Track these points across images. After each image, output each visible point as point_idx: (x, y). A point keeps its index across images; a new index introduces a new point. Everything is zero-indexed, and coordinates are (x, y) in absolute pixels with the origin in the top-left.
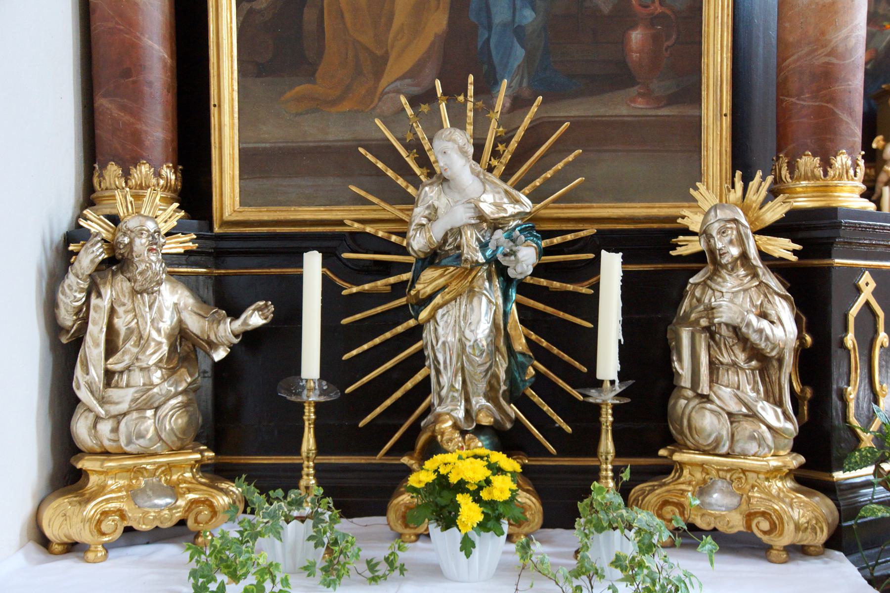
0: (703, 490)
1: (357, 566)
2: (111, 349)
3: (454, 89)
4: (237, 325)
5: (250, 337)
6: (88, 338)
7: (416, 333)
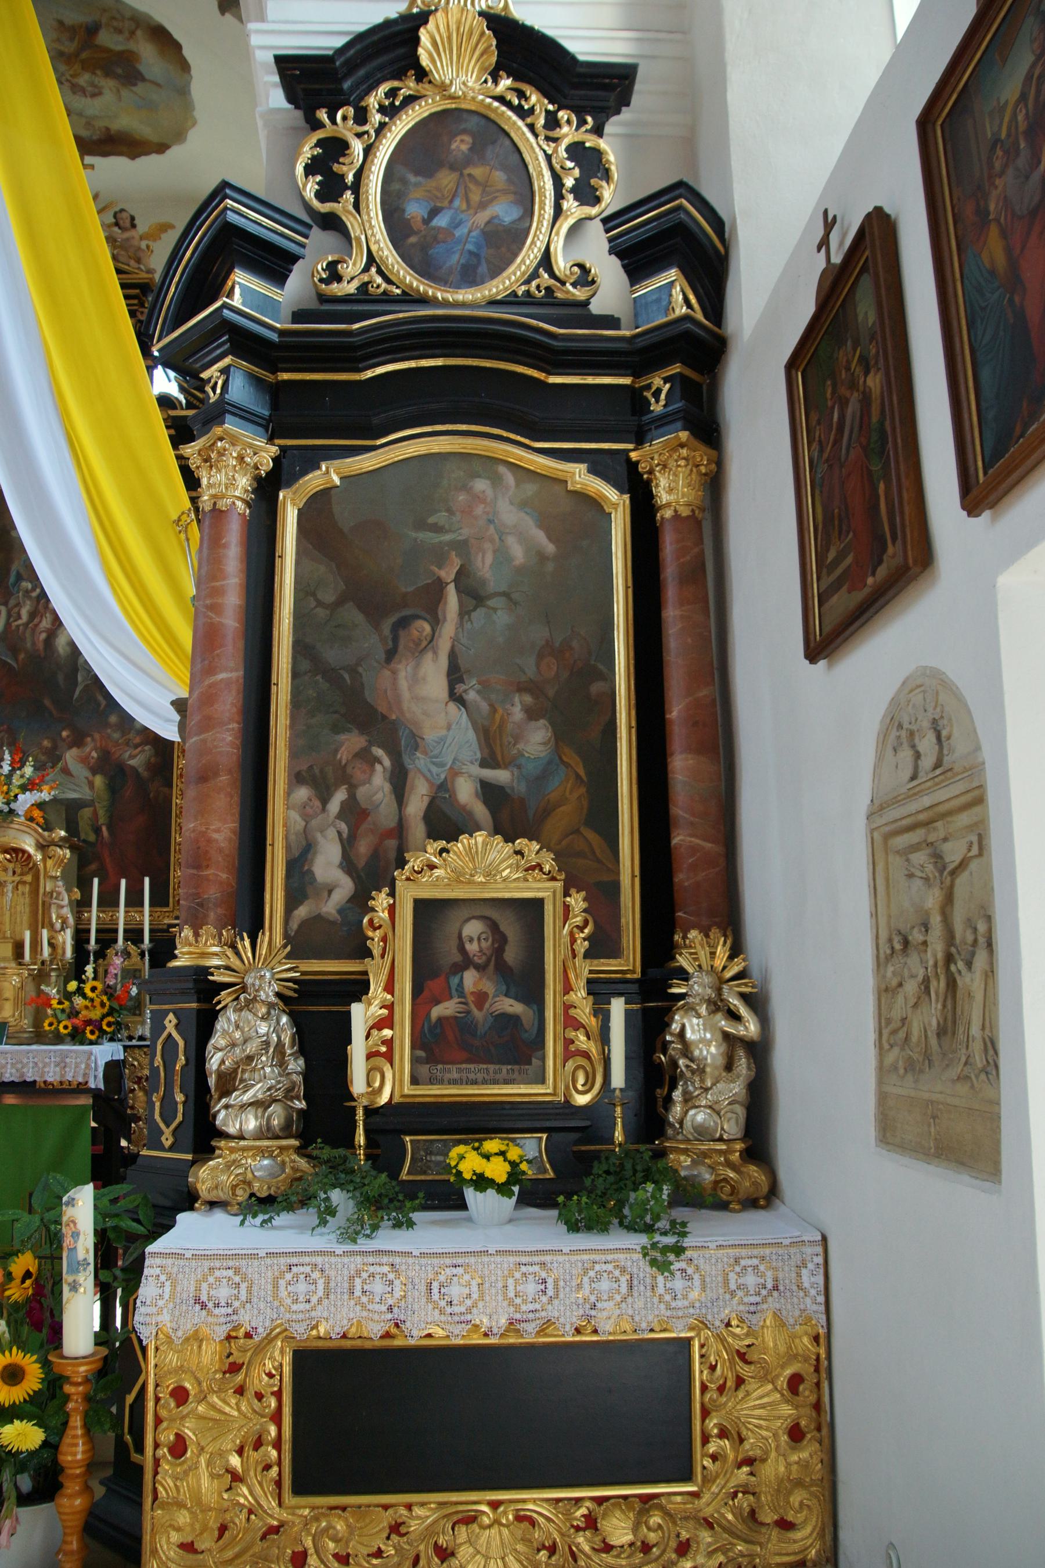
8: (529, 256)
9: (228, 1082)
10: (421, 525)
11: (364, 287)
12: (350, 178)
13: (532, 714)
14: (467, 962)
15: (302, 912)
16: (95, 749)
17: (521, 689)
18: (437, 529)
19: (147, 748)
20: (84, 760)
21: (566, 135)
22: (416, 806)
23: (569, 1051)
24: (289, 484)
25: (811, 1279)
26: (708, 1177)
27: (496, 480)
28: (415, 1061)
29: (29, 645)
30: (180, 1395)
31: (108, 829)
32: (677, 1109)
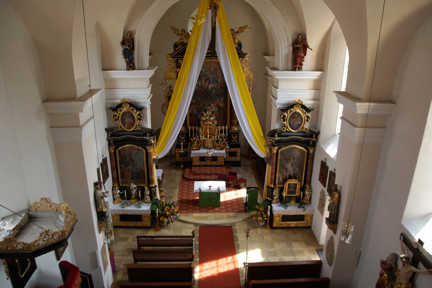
2: (116, 194)
5: (123, 193)
8: (301, 127)
9: (275, 196)
10: (290, 153)
11: (286, 131)
12: (286, 119)
13: (297, 168)
14: (291, 187)
15: (279, 182)
17: (297, 166)
18: (291, 153)
19: (224, 104)
20: (214, 105)
21: (306, 115)
22: (288, 174)
23: (298, 193)
24: (279, 150)
25: (313, 212)
26: (306, 202)
27: (296, 149)
28: (287, 194)
29: (204, 88)
30: (276, 217)
31: (218, 115)
32: (305, 198)
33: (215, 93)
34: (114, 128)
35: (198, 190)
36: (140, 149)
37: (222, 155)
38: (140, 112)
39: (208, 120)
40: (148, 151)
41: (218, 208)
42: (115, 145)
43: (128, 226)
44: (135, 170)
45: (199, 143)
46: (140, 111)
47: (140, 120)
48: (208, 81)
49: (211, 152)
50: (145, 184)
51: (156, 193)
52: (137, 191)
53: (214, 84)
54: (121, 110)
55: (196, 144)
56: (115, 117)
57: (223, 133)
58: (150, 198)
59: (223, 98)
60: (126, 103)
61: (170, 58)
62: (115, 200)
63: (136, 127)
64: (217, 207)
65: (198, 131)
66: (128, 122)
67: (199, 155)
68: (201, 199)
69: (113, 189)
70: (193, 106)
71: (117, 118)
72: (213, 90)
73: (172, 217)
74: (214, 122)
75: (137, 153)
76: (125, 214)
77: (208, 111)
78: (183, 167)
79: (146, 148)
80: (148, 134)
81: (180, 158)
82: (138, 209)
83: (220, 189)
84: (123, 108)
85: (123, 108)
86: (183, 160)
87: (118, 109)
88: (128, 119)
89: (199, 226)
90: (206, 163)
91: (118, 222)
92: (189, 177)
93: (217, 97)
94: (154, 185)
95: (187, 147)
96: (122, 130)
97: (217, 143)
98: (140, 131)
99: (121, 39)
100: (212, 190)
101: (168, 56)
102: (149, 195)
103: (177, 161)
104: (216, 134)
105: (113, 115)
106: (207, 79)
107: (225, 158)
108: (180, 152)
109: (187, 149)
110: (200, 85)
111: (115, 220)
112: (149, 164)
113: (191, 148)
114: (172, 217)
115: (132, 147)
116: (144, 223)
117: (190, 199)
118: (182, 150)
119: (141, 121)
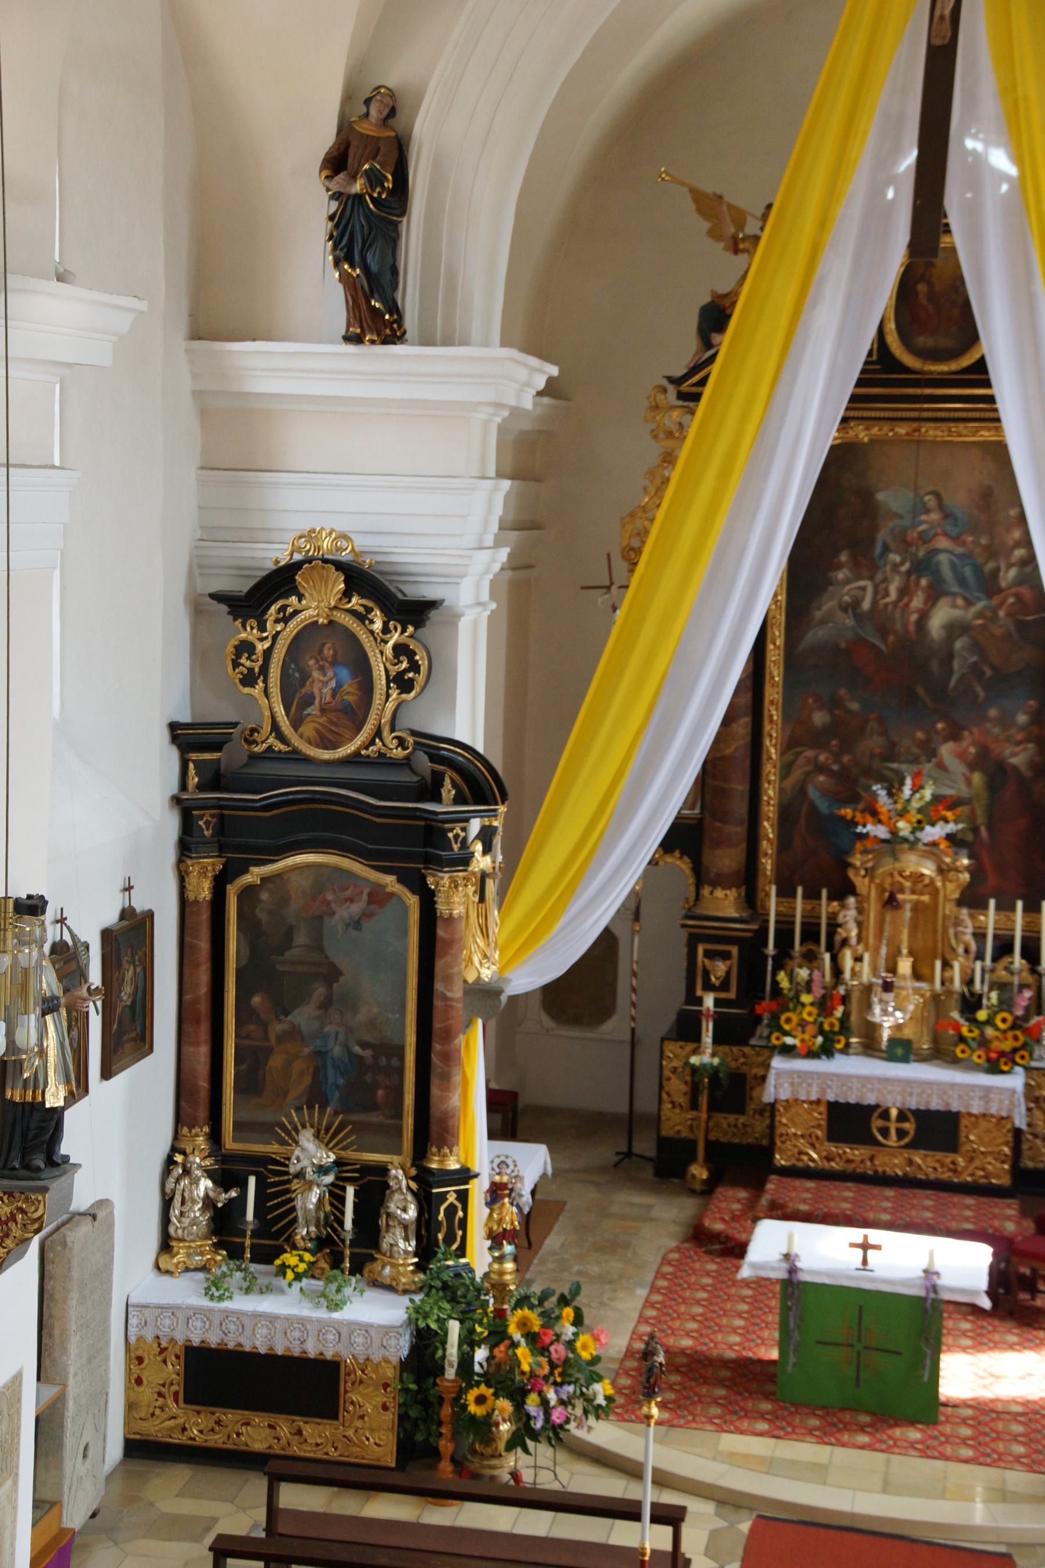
0: (383, 1267)
1: (256, 1288)
2: (183, 1203)
3: (311, 1108)
4: (227, 1196)
5: (231, 1200)
6: (175, 1201)
7: (292, 1200)
16: (974, 743)
19: (1031, 745)
20: (961, 755)
29: (898, 626)
33: (975, 664)
34: (235, 725)
35: (775, 1265)
36: (389, 889)
37: (1000, 1109)
38: (411, 636)
39: (905, 840)
40: (441, 907)
41: (920, 1426)
42: (222, 849)
43: (230, 1446)
44: (341, 1037)
45: (834, 1008)
46: (411, 629)
47: (405, 685)
48: (924, 582)
49: (892, 1014)
50: (398, 1151)
51: (463, 1224)
52: (337, 1197)
53: (969, 603)
54: (290, 610)
55: (808, 1009)
56: (243, 661)
57: (1017, 960)
58: (416, 1255)
59: (1032, 703)
60: (325, 561)
61: (675, 414)
62: (173, 1243)
63: (378, 733)
64: (912, 1423)
65: (834, 925)
66: (328, 698)
67: (823, 1091)
68: (796, 1335)
69: (170, 1162)
70: (809, 753)
71: (260, 663)
72: (959, 644)
73: (556, 1392)
74: (948, 860)
75: (366, 915)
76: (223, 1343)
77: (908, 782)
78: (705, 1175)
79: (430, 880)
80: (447, 782)
81: (690, 1115)
82: (322, 1314)
83: (937, 1274)
84: (300, 601)
85: (300, 601)
86: (707, 1131)
87: (268, 608)
88: (325, 676)
89: (754, 1515)
90: (872, 1159)
91: (162, 1408)
92: (730, 1232)
93: (982, 694)
94: (458, 1161)
95: (752, 1034)
96: (280, 752)
97: (962, 1021)
98: (402, 765)
99: (326, 137)
100: (879, 1273)
101: (661, 397)
102: (413, 1228)
103: (664, 1133)
104: (961, 950)
105: (236, 647)
106: (923, 566)
107: (1017, 1133)
108: (694, 1060)
109: (747, 1050)
110: (866, 605)
111: (146, 1394)
112: (437, 1003)
113: (775, 1035)
114: (552, 1396)
115: (337, 869)
116: (350, 1433)
117: (715, 1353)
118: (709, 1051)
119: (413, 694)
